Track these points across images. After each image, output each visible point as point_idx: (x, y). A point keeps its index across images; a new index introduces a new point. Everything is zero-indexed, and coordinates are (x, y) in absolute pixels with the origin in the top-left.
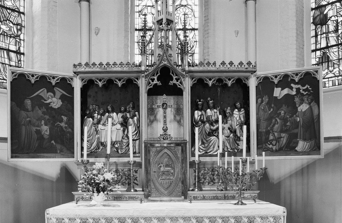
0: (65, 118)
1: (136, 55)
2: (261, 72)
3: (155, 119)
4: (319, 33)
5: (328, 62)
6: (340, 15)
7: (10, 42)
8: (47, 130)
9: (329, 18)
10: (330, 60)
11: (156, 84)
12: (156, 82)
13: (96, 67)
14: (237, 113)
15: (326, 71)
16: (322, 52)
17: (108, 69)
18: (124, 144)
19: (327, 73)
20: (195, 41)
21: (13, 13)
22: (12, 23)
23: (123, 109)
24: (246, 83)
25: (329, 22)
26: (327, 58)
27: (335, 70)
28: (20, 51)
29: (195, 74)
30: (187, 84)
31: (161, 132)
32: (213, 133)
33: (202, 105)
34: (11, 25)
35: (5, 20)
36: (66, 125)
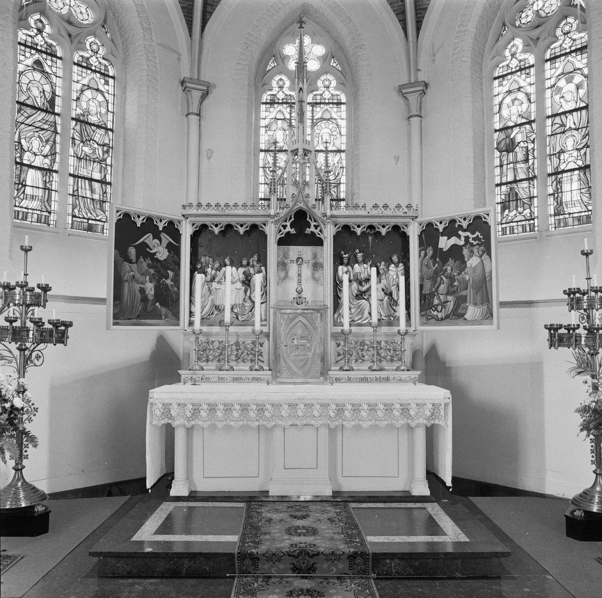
0: (171, 273)
1: (260, 185)
2: (426, 218)
3: (286, 277)
5: (517, 200)
7: (94, 167)
8: (151, 289)
10: (519, 198)
11: (289, 232)
12: (288, 229)
13: (211, 208)
14: (394, 269)
15: (514, 212)
16: (508, 187)
17: (227, 212)
18: (246, 308)
20: (341, 167)
21: (98, 131)
22: (97, 144)
23: (245, 262)
24: (405, 231)
25: (517, 149)
26: (514, 195)
27: (525, 212)
28: (106, 180)
29: (339, 220)
30: (328, 233)
31: (295, 295)
32: (362, 295)
33: (349, 258)
34: (96, 146)
35: (88, 140)
36: (172, 283)
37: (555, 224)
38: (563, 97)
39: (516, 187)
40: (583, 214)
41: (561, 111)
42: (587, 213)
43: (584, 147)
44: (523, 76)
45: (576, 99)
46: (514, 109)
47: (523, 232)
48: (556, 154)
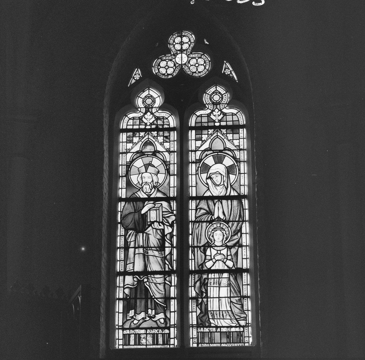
4: (132, 244)
6: (168, 223)
9: (149, 223)
10: (149, 297)
15: (143, 315)
19: (143, 318)
25: (150, 230)
26: (143, 292)
27: (158, 317)
37: (197, 338)
38: (210, 178)
39: (146, 280)
40: (233, 329)
41: (208, 194)
42: (237, 329)
43: (234, 246)
44: (161, 139)
45: (226, 185)
46: (147, 177)
47: (153, 344)
48: (200, 247)
